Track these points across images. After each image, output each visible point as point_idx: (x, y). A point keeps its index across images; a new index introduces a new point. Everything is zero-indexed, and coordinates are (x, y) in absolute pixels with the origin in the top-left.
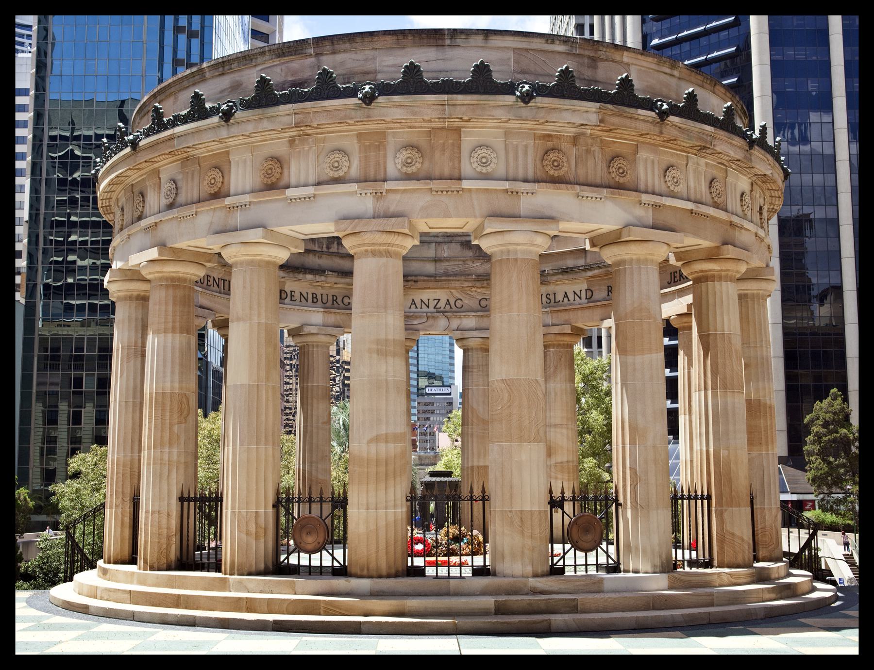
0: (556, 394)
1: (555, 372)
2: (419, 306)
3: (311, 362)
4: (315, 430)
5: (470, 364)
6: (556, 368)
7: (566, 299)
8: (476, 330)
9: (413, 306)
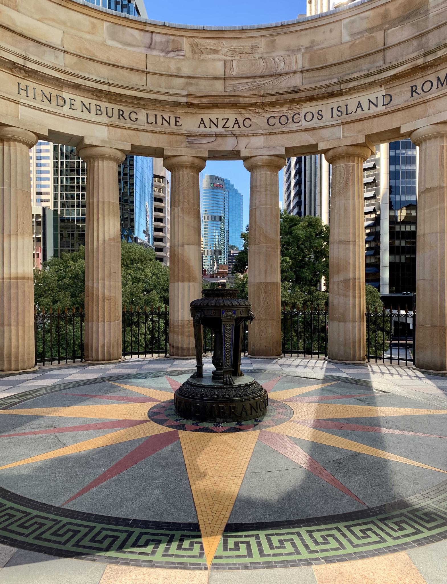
2: (207, 125)
7: (360, 109)
8: (264, 148)
9: (202, 125)
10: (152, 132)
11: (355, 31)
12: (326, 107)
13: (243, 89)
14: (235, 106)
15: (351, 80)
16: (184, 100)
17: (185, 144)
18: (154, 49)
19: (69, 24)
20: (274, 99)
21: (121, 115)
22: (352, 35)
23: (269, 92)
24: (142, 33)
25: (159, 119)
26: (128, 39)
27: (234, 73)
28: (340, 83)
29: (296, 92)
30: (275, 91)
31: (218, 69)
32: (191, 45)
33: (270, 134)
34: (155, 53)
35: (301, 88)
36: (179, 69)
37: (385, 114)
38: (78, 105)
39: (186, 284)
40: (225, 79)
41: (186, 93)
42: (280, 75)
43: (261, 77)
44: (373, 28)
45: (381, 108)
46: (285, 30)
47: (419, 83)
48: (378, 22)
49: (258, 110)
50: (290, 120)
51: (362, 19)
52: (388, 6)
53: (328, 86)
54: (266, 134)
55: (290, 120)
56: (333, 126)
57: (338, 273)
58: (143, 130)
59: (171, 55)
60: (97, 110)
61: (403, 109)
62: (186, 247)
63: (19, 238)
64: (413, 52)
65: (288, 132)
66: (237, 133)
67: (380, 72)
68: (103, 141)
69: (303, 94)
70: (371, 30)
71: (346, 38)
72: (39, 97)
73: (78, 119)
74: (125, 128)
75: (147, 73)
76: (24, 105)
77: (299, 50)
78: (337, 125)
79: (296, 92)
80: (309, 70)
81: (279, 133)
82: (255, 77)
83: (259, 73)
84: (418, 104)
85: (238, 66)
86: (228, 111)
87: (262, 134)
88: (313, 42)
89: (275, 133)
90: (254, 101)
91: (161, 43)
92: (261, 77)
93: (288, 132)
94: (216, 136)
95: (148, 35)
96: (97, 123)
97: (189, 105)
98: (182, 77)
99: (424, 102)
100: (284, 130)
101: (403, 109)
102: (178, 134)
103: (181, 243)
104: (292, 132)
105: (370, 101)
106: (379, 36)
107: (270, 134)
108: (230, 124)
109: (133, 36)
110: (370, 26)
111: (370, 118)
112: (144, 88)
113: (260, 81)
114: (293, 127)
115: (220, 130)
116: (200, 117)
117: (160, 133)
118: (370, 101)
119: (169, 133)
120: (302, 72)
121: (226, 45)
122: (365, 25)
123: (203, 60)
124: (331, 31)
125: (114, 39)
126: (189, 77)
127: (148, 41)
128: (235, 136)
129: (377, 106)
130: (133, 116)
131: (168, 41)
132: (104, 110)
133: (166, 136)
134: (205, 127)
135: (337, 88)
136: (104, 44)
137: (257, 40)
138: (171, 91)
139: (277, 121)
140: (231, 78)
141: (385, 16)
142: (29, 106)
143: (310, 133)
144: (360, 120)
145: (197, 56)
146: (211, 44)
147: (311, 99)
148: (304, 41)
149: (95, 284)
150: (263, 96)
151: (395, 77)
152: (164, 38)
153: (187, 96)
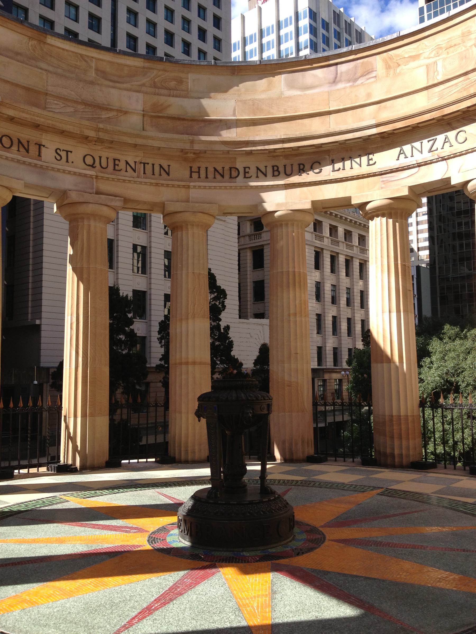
18: (340, 81)
34: (340, 86)
38: (253, 171)
60: (274, 171)
72: (211, 176)
127: (332, 77)
128: (444, 159)
131: (356, 67)
134: (406, 157)
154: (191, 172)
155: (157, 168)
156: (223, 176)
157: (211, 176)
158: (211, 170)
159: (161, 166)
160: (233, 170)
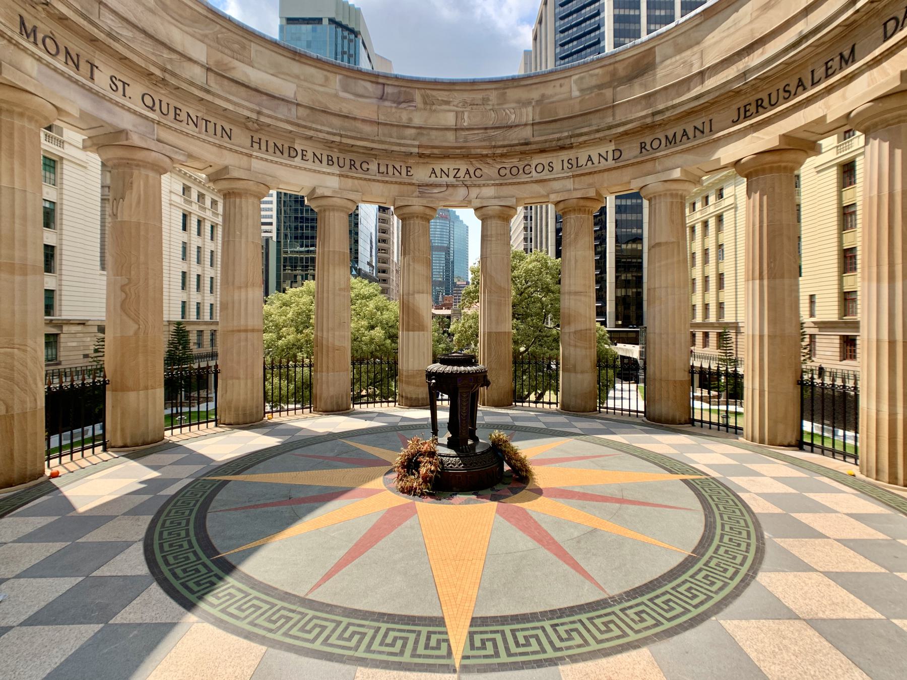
0: (576, 261)
1: (575, 238)
2: (439, 175)
3: (327, 227)
4: (331, 296)
5: (489, 233)
6: (577, 235)
7: (590, 163)
8: (495, 198)
9: (433, 175)
10: (383, 182)
11: (585, 86)
12: (558, 160)
13: (475, 141)
14: (467, 156)
15: (581, 135)
16: (416, 150)
17: (417, 193)
18: (386, 100)
19: (302, 78)
20: (505, 150)
21: (352, 165)
22: (582, 90)
23: (501, 143)
24: (374, 85)
25: (390, 169)
26: (360, 91)
27: (465, 124)
28: (571, 137)
29: (527, 144)
30: (506, 143)
31: (449, 119)
32: (422, 96)
33: (501, 184)
34: (387, 104)
35: (532, 140)
36: (410, 119)
37: (615, 168)
38: (310, 155)
39: (416, 333)
40: (456, 130)
41: (417, 143)
42: (511, 127)
43: (492, 128)
44: (602, 84)
45: (611, 163)
46: (515, 84)
47: (648, 141)
48: (607, 79)
49: (489, 161)
50: (521, 171)
51: (592, 76)
52: (616, 65)
53: (559, 139)
54: (497, 185)
55: (521, 171)
56: (563, 178)
57: (569, 324)
58: (374, 180)
59: (403, 105)
61: (633, 164)
62: (416, 296)
63: (250, 289)
64: (642, 110)
65: (519, 183)
66: (468, 183)
67: (610, 128)
68: (334, 191)
69: (534, 147)
70: (600, 87)
71: (576, 93)
72: (271, 150)
73: (310, 170)
74: (356, 178)
75: (379, 123)
76: (257, 157)
77: (529, 103)
78: (568, 177)
79: (527, 144)
80: (540, 123)
81: (511, 184)
82: (486, 129)
83: (490, 124)
84: (647, 161)
85: (469, 117)
86: (459, 162)
87: (493, 185)
88: (543, 96)
89: (506, 184)
90: (485, 152)
91: (393, 94)
92: (492, 128)
93: (519, 183)
94: (448, 186)
95: (380, 87)
96: (329, 174)
97: (421, 156)
98: (414, 127)
99: (654, 159)
100: (515, 181)
101: (633, 164)
102: (410, 184)
103: (411, 292)
104: (523, 183)
105: (600, 155)
106: (608, 93)
107: (501, 184)
108: (461, 174)
109: (365, 88)
110: (599, 82)
111: (600, 171)
112: (376, 138)
113: (492, 133)
114: (523, 178)
115: (451, 179)
116: (431, 166)
117: (392, 183)
118: (600, 155)
119: (400, 183)
120: (533, 124)
121: (458, 97)
122: (594, 82)
123: (435, 111)
124: (561, 86)
125: (346, 91)
126: (420, 128)
127: (379, 92)
129: (607, 160)
130: (365, 166)
131: (400, 93)
132: (335, 160)
133: (397, 186)
135: (568, 142)
136: (336, 96)
137: (488, 92)
138: (402, 142)
139: (508, 171)
140: (462, 129)
141: (614, 74)
142: (262, 159)
143: (541, 184)
144: (590, 173)
145: (428, 107)
146: (442, 95)
147: (542, 151)
148: (535, 94)
149: (325, 333)
150: (495, 147)
151: (626, 133)
152: (396, 90)
153: (419, 146)
154: (252, 141)
155: (219, 129)
156: (282, 153)
157: (271, 150)
158: (271, 144)
159: (223, 128)
160: (292, 150)
